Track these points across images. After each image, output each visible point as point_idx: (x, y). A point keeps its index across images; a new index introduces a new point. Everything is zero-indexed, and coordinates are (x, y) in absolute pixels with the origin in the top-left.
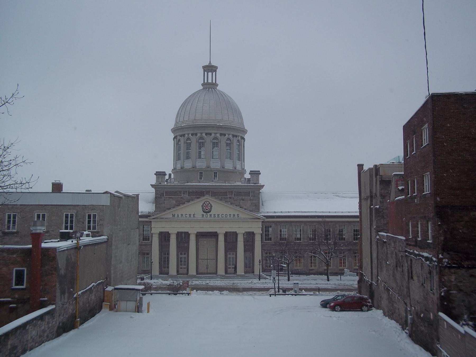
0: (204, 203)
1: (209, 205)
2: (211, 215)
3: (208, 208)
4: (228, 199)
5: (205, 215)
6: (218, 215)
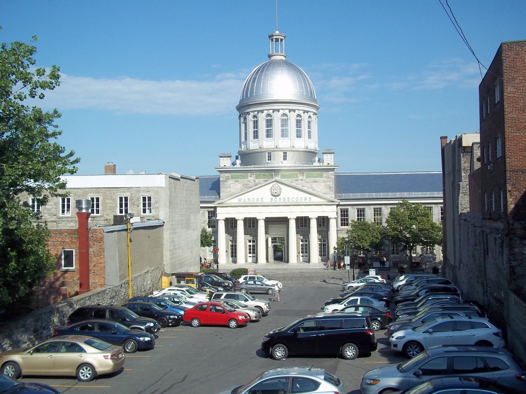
0: (273, 186)
1: (278, 187)
2: (280, 199)
3: (277, 192)
4: (299, 182)
5: (274, 199)
6: (288, 198)
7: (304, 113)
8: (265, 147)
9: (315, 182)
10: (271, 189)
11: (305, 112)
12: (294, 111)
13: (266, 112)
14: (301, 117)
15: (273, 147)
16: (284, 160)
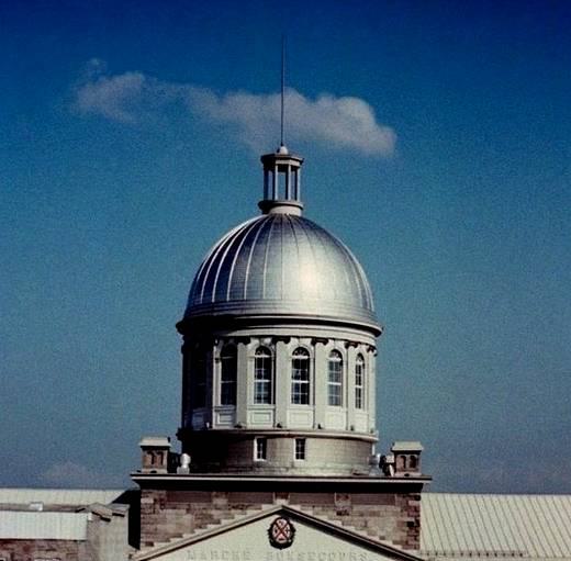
0: (275, 523)
7: (347, 347)
8: (250, 427)
9: (374, 514)
10: (270, 531)
11: (348, 344)
12: (325, 341)
13: (254, 343)
14: (340, 356)
15: (270, 427)
16: (297, 458)
